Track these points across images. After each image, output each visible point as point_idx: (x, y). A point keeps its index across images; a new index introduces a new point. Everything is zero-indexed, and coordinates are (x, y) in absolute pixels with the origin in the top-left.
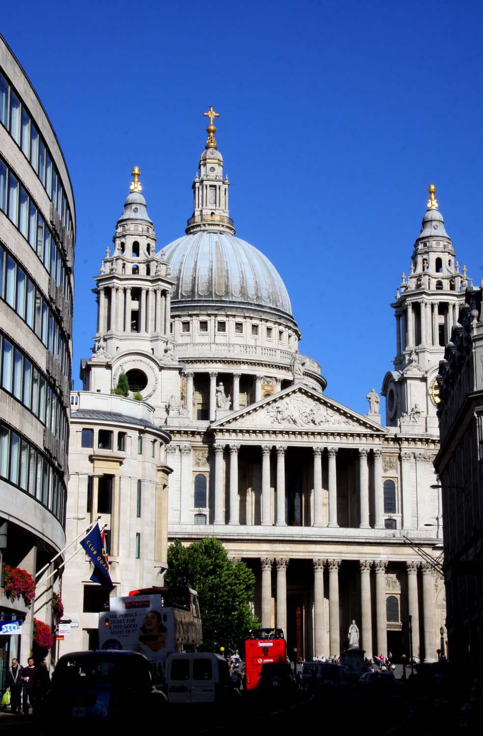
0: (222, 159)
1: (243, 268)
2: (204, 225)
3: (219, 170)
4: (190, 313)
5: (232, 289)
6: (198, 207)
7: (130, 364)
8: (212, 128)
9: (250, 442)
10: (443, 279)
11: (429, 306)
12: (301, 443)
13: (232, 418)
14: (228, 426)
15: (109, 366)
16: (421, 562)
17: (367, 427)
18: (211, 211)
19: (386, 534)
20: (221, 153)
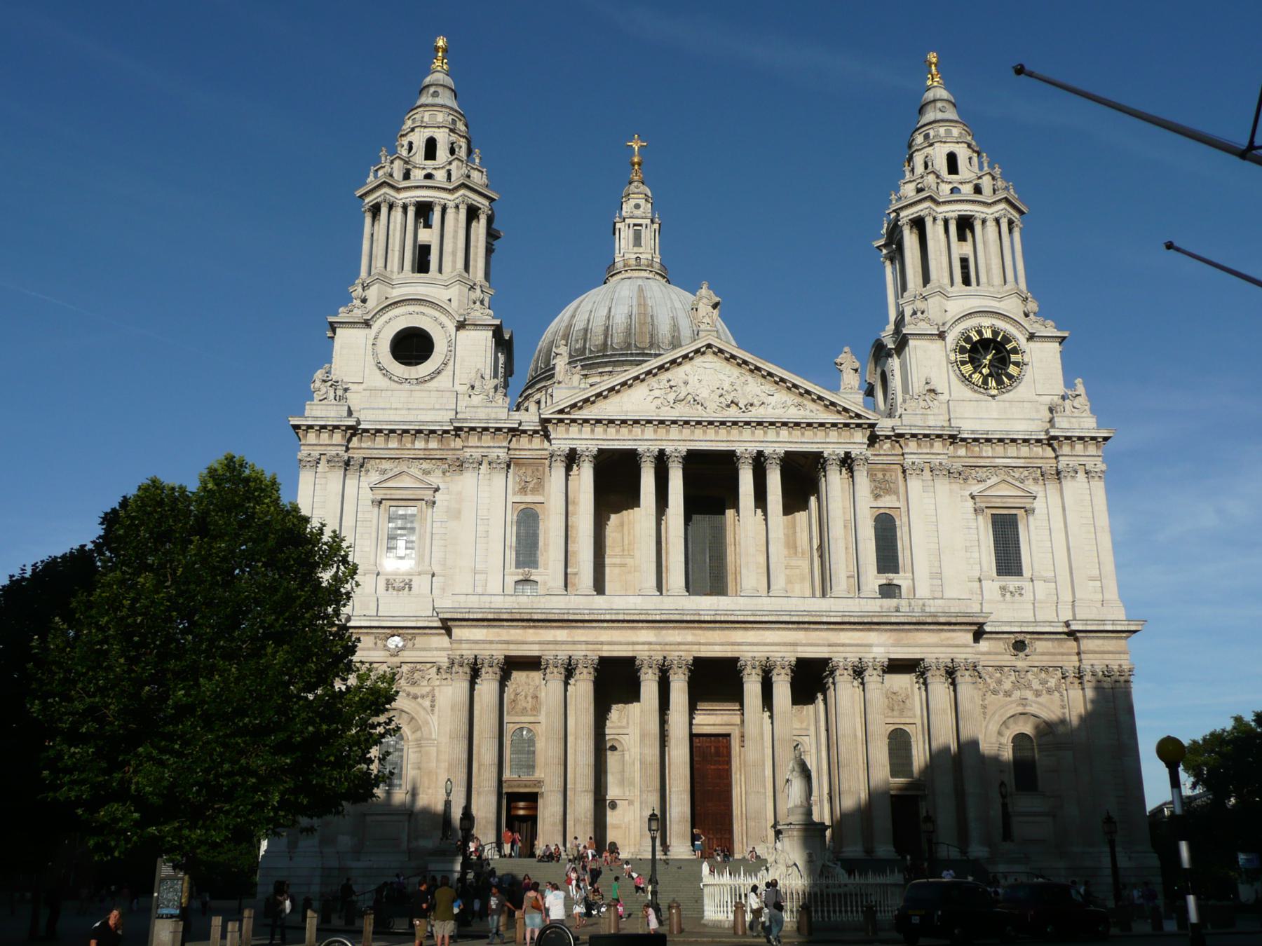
0: (650, 195)
2: (626, 271)
3: (646, 208)
4: (600, 370)
5: (658, 338)
7: (401, 320)
8: (636, 160)
9: (616, 443)
10: (961, 183)
11: (940, 224)
12: (713, 444)
13: (581, 398)
14: (576, 415)
15: (367, 324)
16: (952, 660)
17: (839, 412)
18: (636, 256)
19: (881, 607)
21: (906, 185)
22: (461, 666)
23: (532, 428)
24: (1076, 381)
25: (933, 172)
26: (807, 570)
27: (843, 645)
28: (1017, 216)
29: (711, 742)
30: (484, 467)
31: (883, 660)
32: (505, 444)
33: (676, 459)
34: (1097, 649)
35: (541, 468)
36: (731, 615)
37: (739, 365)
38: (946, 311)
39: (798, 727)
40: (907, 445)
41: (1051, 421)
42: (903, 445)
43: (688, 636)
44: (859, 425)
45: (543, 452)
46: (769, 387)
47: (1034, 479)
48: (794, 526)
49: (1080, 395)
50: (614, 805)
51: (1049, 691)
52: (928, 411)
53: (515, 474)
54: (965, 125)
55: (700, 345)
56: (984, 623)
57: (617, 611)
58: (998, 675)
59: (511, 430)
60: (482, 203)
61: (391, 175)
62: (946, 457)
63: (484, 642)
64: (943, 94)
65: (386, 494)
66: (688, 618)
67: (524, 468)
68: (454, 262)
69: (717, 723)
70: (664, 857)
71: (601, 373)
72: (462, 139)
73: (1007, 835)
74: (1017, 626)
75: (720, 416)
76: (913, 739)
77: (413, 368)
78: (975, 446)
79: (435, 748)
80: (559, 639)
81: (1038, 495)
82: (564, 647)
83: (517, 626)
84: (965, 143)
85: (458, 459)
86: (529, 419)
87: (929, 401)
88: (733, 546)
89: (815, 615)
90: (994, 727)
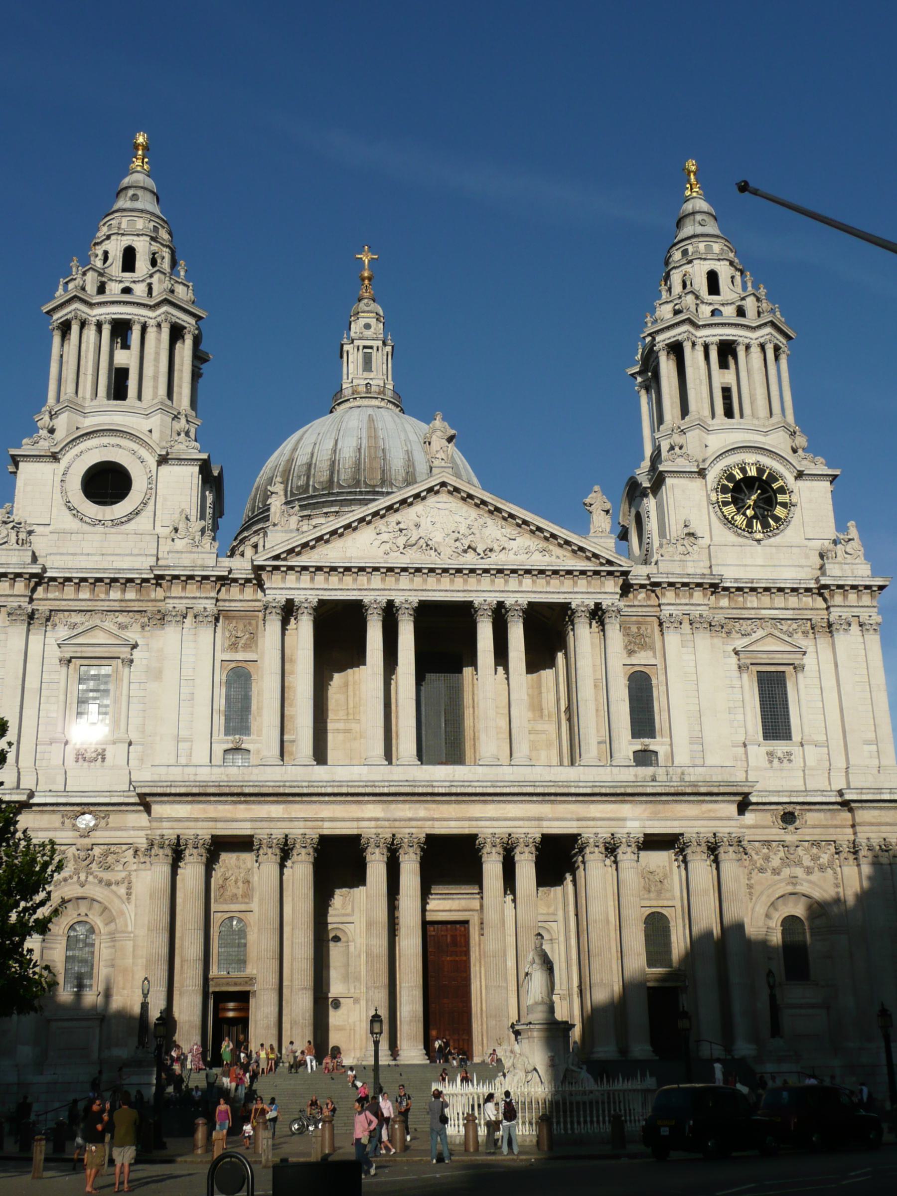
0: (382, 314)
1: (409, 446)
2: (355, 398)
3: (377, 328)
4: (325, 510)
5: (390, 475)
6: (348, 379)
8: (366, 274)
9: (339, 593)
10: (723, 305)
11: (700, 349)
12: (449, 594)
14: (294, 561)
15: (55, 457)
16: (715, 834)
17: (588, 558)
18: (366, 382)
19: (636, 776)
20: (381, 306)
21: (663, 307)
22: (162, 848)
23: (244, 576)
24: (849, 524)
25: (692, 292)
26: (554, 736)
27: (594, 819)
28: (784, 341)
29: (447, 930)
30: (189, 620)
31: (638, 836)
32: (213, 594)
33: (406, 611)
34: (874, 821)
35: (254, 622)
36: (469, 786)
37: (477, 505)
38: (706, 446)
39: (545, 912)
40: (663, 594)
41: (822, 568)
42: (659, 595)
43: (421, 810)
44: (610, 573)
45: (257, 604)
46: (510, 530)
47: (803, 633)
48: (539, 686)
49: (853, 539)
50: (337, 1004)
51: (822, 869)
52: (687, 557)
53: (224, 629)
54: (726, 240)
55: (433, 484)
56: (749, 794)
57: (340, 783)
58: (765, 851)
59: (220, 578)
60: (188, 321)
61: (83, 289)
62: (706, 608)
63: (188, 819)
64: (702, 205)
65: (76, 652)
66: (420, 790)
67: (234, 622)
68: (156, 388)
69: (453, 908)
70: (393, 1063)
71: (326, 513)
72: (164, 249)
73: (776, 1030)
74: (786, 796)
75: (456, 562)
76: (672, 924)
77: (108, 509)
78: (739, 596)
79: (132, 942)
80: (274, 816)
81: (808, 651)
82: (279, 824)
83: (226, 801)
84: (727, 260)
85: (159, 611)
86: (241, 566)
87: (688, 546)
88: (471, 709)
89: (562, 786)
90: (761, 909)
